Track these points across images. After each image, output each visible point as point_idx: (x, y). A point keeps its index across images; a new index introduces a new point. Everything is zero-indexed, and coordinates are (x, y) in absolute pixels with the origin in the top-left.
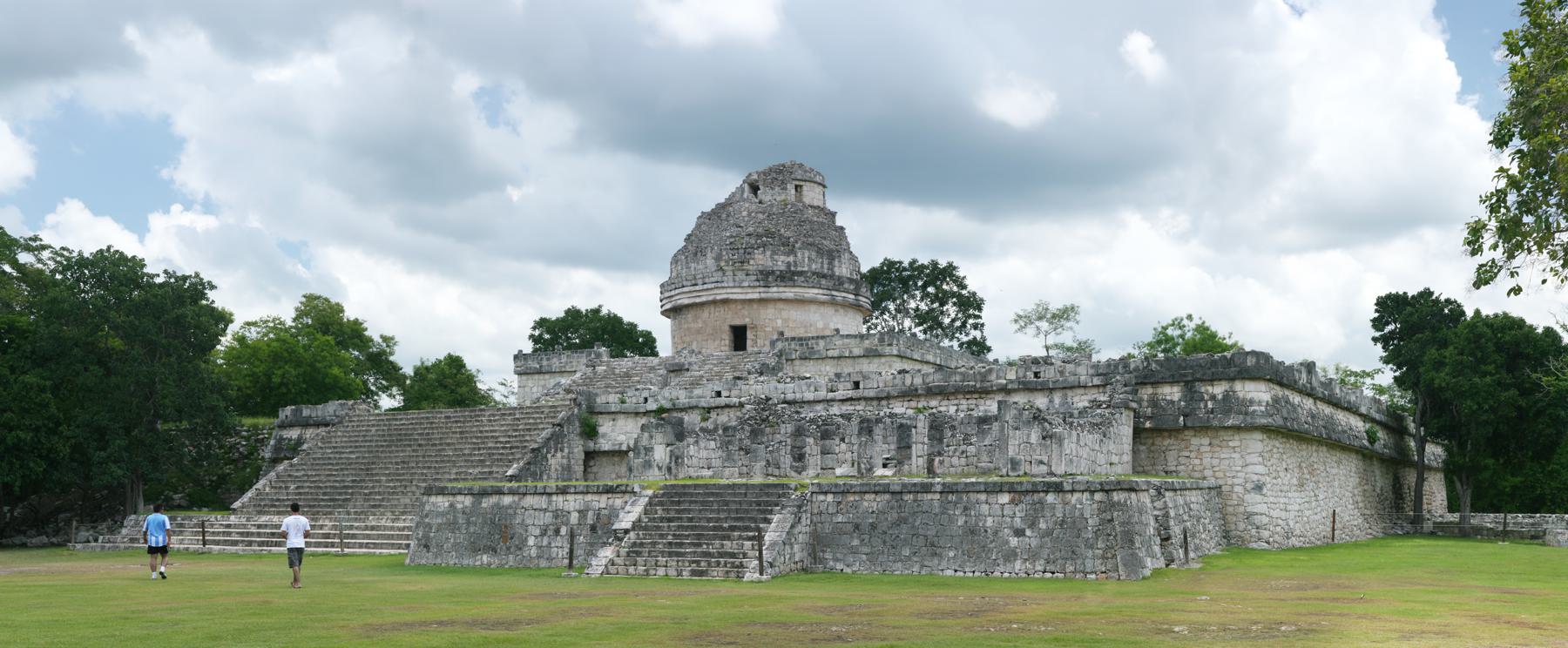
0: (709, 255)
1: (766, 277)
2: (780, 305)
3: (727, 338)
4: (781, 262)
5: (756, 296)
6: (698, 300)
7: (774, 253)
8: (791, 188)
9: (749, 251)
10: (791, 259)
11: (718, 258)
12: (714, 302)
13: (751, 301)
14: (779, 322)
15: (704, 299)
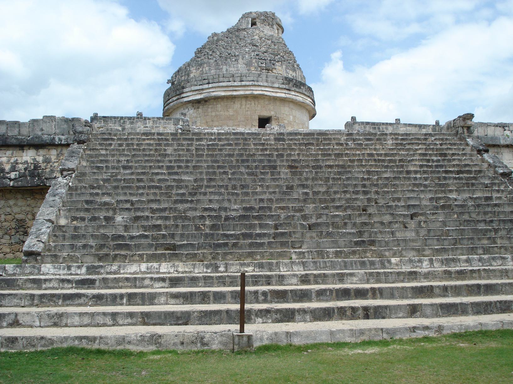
0: (240, 61)
1: (288, 80)
2: (291, 105)
3: (257, 124)
4: (291, 74)
5: (283, 95)
6: (235, 93)
7: (287, 68)
8: (275, 27)
9: (272, 62)
10: (294, 74)
11: (249, 64)
12: (246, 97)
13: (275, 99)
14: (291, 117)
15: (242, 93)
